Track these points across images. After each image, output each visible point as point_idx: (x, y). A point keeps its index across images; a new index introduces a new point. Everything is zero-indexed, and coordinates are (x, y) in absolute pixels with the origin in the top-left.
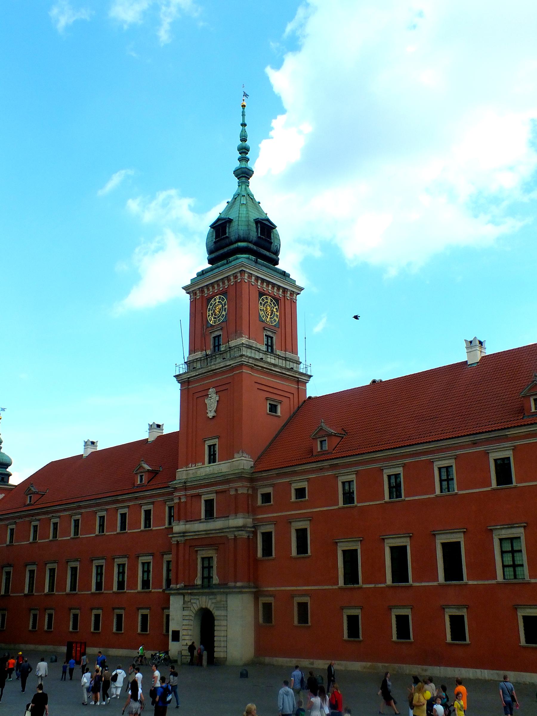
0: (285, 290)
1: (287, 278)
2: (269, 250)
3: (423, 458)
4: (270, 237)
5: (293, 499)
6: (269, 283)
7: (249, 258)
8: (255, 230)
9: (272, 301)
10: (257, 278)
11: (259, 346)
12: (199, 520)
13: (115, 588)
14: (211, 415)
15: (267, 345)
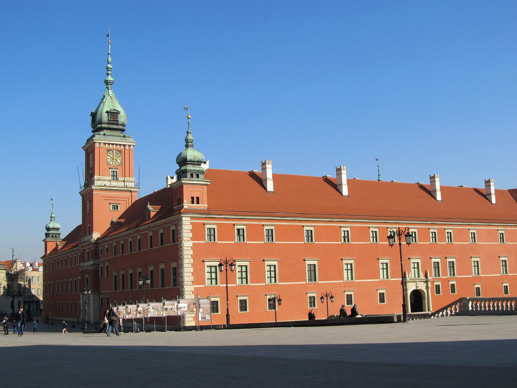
0: (124, 145)
1: (127, 138)
2: (118, 124)
3: (127, 237)
4: (117, 118)
5: (106, 253)
6: (113, 144)
7: (99, 134)
8: (107, 117)
9: (116, 152)
10: (105, 144)
11: (106, 178)
12: (85, 261)
13: (74, 292)
14: (88, 212)
15: (113, 176)
